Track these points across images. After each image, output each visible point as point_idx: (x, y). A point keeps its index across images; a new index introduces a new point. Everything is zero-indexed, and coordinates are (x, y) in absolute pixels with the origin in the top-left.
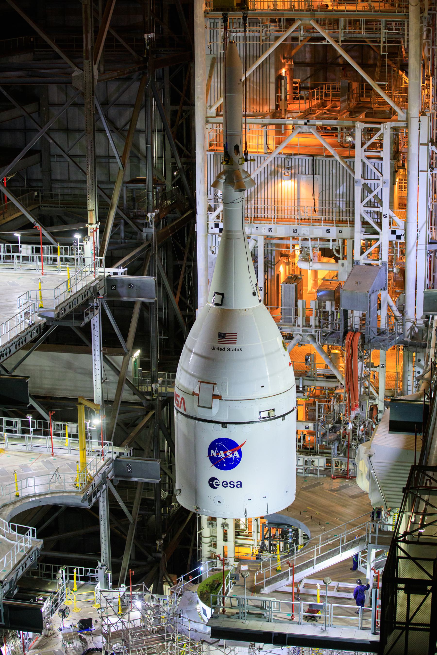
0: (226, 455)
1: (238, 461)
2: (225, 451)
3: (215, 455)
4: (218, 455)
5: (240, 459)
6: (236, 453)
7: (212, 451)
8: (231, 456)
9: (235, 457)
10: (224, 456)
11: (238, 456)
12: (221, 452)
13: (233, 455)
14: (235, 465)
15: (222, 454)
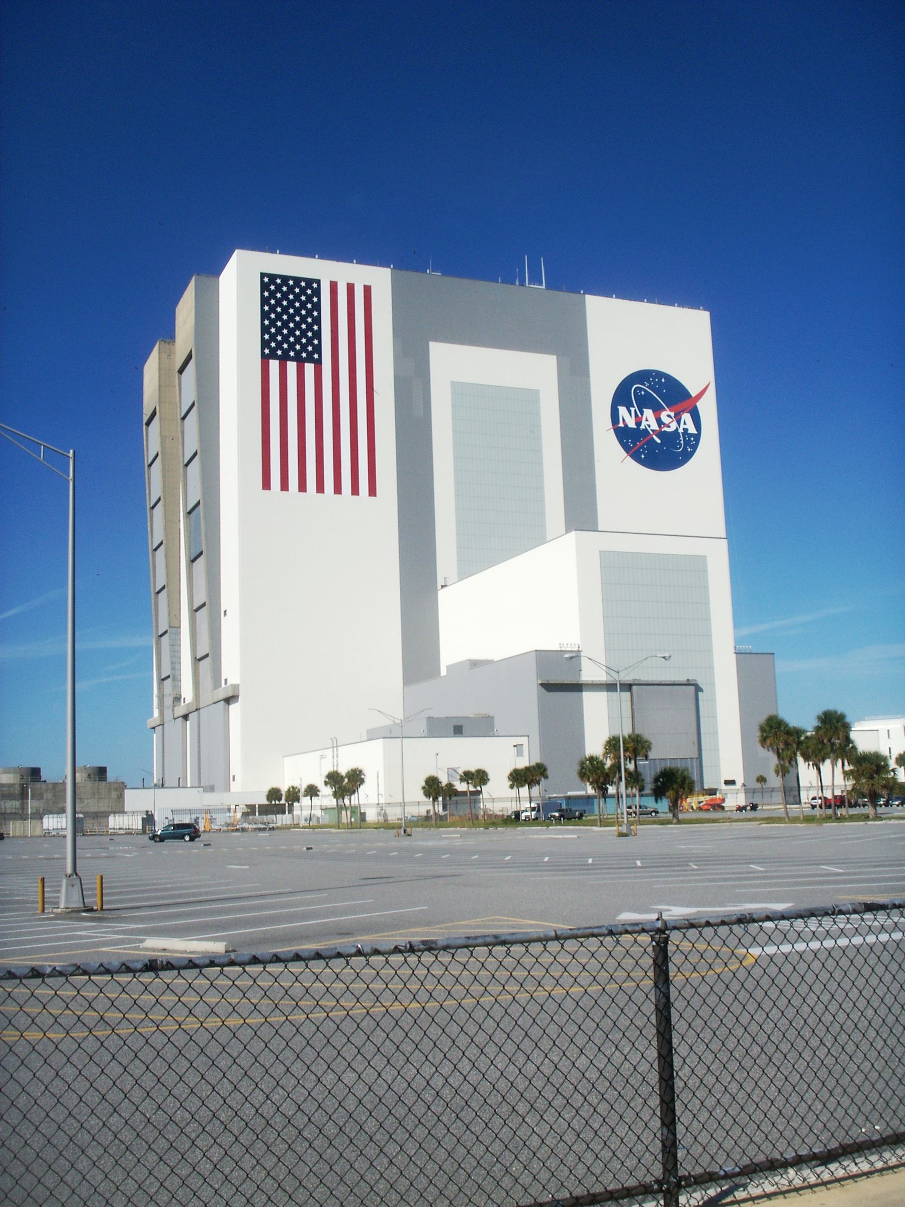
0: (659, 422)
1: (692, 442)
2: (657, 410)
3: (631, 424)
4: (638, 423)
5: (697, 437)
6: (686, 417)
7: (622, 411)
8: (673, 426)
9: (685, 430)
10: (655, 426)
11: (692, 430)
12: (648, 413)
13: (679, 422)
14: (686, 456)
15: (649, 418)
